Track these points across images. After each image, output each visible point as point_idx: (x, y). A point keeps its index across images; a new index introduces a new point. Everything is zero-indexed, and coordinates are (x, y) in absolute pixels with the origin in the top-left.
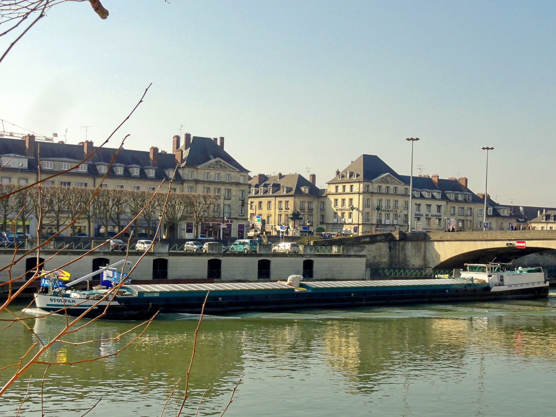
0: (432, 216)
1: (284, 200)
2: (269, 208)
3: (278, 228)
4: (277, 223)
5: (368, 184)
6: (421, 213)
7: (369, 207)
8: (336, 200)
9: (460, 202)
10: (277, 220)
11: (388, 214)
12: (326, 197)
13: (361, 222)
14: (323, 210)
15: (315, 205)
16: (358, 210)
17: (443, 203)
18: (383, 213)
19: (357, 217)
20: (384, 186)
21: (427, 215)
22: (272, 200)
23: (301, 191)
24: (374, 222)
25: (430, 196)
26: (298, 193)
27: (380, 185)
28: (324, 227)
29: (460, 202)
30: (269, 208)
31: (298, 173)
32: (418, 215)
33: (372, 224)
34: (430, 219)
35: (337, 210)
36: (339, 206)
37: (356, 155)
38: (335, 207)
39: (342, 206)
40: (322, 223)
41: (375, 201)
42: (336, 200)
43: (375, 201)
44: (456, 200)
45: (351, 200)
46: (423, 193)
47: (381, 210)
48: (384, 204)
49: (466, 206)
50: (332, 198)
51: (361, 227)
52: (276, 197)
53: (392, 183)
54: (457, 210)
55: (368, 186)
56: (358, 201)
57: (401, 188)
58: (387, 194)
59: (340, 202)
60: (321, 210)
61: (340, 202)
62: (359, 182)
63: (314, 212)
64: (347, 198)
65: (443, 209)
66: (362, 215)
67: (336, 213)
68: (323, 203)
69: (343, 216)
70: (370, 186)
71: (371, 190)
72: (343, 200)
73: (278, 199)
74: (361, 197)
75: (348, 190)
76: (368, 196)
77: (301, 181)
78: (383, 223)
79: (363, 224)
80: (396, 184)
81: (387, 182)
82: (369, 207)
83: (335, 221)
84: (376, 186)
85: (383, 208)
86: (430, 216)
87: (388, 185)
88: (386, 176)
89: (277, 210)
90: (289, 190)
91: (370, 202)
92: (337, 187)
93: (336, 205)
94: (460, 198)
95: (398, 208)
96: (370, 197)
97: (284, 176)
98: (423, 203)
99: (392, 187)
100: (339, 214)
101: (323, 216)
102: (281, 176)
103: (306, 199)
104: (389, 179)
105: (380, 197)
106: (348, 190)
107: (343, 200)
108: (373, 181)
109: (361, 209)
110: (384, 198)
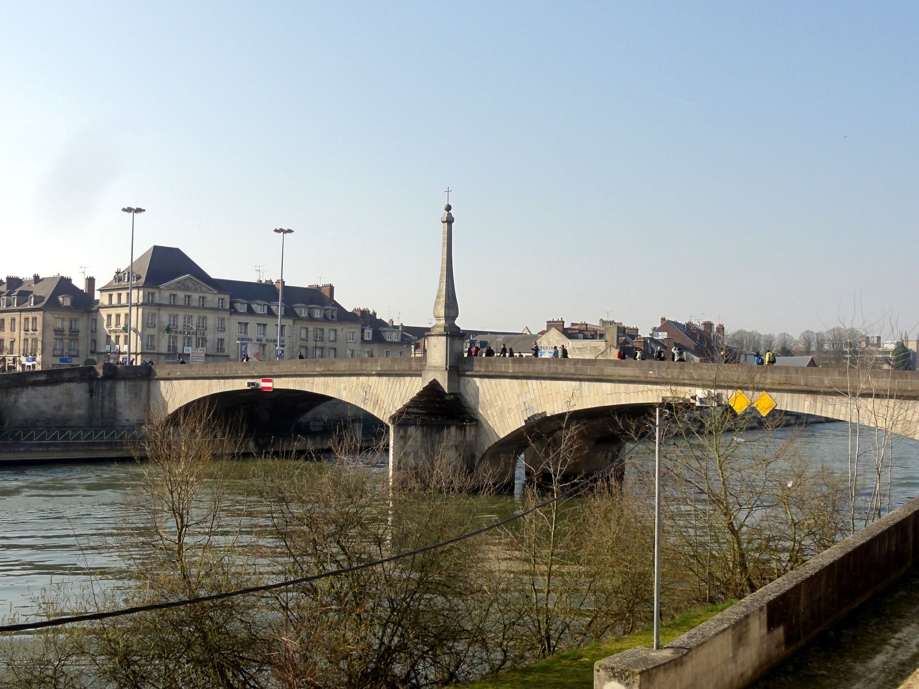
0: (267, 340)
1: (30, 315)
2: (13, 330)
3: (23, 359)
4: (22, 352)
5: (151, 290)
6: (249, 335)
7: (154, 327)
8: (109, 316)
9: (317, 320)
10: (22, 347)
11: (189, 338)
12: (97, 311)
13: (139, 351)
14: (94, 331)
15: (82, 324)
16: (136, 331)
17: (288, 322)
18: (180, 338)
19: (136, 345)
20: (181, 295)
21: (258, 340)
22: (16, 315)
23: (58, 301)
24: (164, 349)
25: (266, 312)
26: (52, 304)
27: (174, 292)
28: (95, 358)
29: (317, 320)
30: (13, 330)
31: (61, 275)
32: (243, 339)
33: (159, 354)
34: (264, 346)
35: (110, 331)
36: (113, 327)
37: (143, 248)
38: (108, 326)
39: (116, 326)
40: (92, 352)
41: (165, 317)
42: (109, 316)
43: (165, 317)
44: (311, 318)
45: (128, 316)
46: (254, 306)
47: (176, 332)
48: (180, 322)
49: (327, 328)
50: (104, 313)
51: (139, 357)
52: (21, 311)
53: (196, 290)
54: (311, 334)
55: (153, 294)
56: (136, 317)
57: (213, 298)
58: (188, 306)
59: (114, 318)
60: (92, 332)
61: (114, 318)
62: (138, 288)
63: (81, 335)
64: (123, 312)
65: (286, 329)
66: (141, 340)
67: (109, 337)
68: (96, 320)
69: (117, 342)
70: (157, 295)
71: (157, 299)
72: (118, 316)
73: (24, 315)
74: (140, 310)
75: (124, 300)
76: (152, 310)
77: (64, 284)
78: (179, 351)
79: (141, 353)
80: (202, 292)
81: (187, 289)
82: (154, 327)
83: (108, 348)
84: (166, 294)
85: (180, 328)
86: (264, 342)
87: (188, 294)
88: (185, 280)
89: (23, 332)
90: (38, 300)
91: (157, 320)
92: (111, 296)
93: (109, 324)
94: (317, 314)
95: (206, 329)
96: (157, 312)
97: (43, 279)
98: (252, 322)
99: (196, 296)
100: (113, 338)
101: (94, 341)
102: (37, 279)
103: (67, 315)
104: (190, 284)
105: (174, 312)
106: (124, 300)
107: (118, 316)
108: (162, 286)
109: (140, 330)
110: (181, 314)
